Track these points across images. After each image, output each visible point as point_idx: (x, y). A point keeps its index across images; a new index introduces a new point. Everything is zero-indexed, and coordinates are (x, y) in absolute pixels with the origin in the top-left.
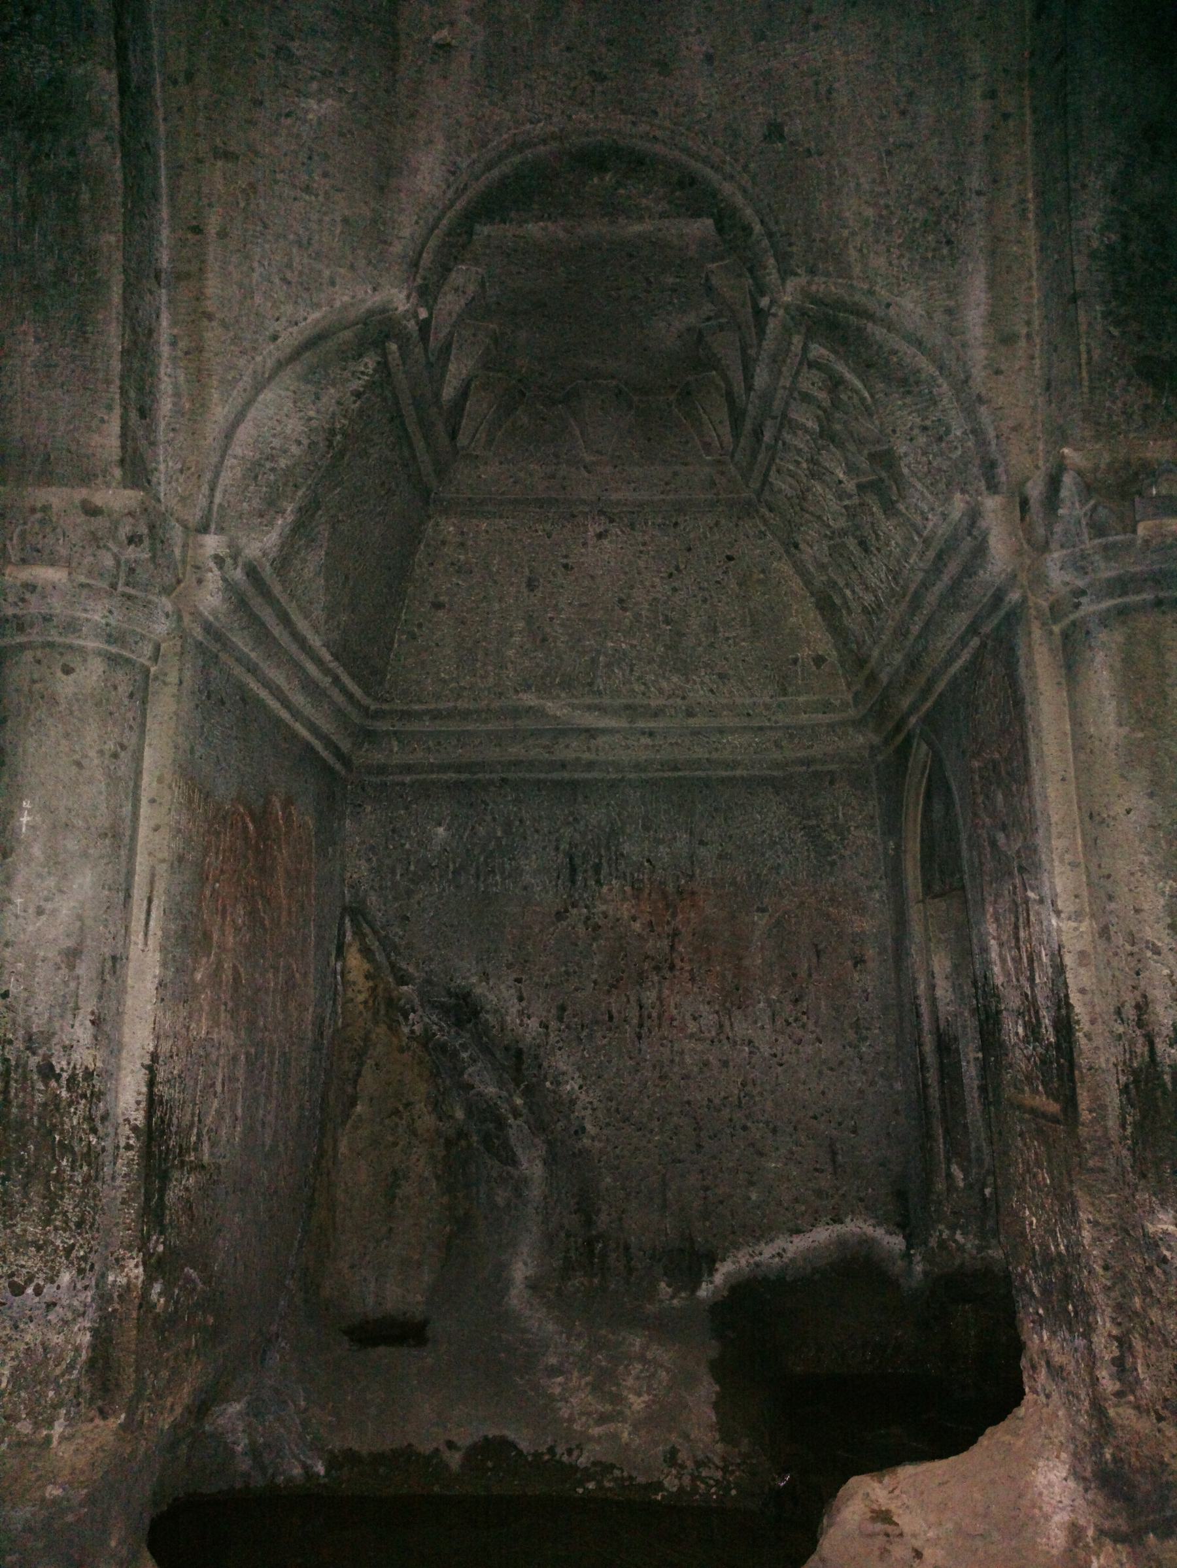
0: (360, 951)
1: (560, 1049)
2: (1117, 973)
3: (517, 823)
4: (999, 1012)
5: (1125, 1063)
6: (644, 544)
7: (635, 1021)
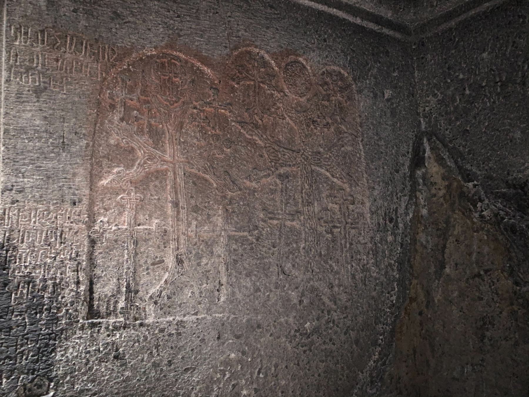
0: (436, 161)
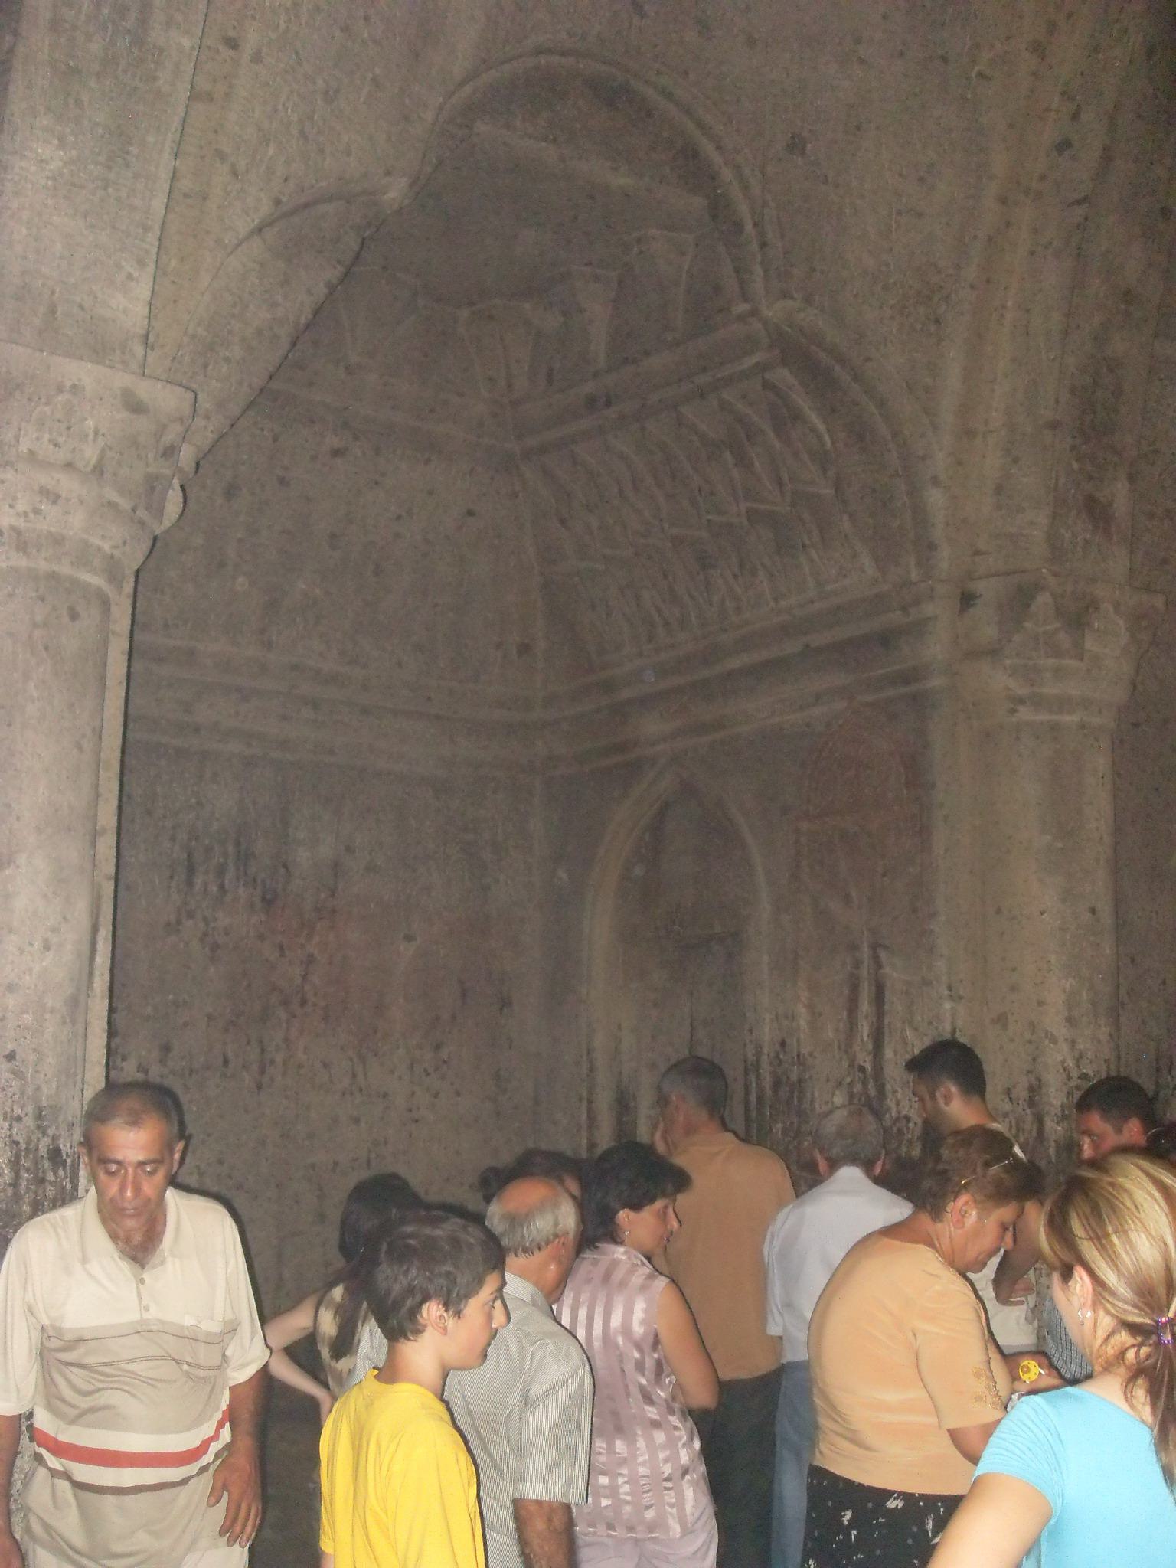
7: (255, 1067)
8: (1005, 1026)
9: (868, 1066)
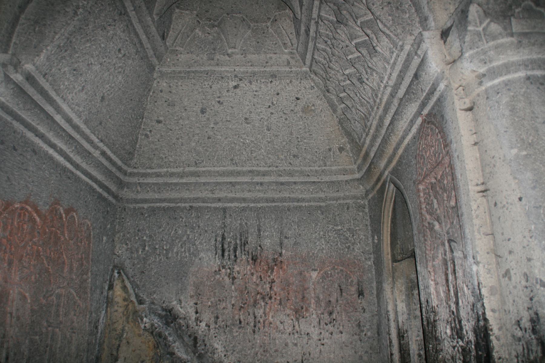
0: (122, 288)
1: (215, 337)
2: (516, 299)
3: (197, 228)
4: (435, 321)
5: (524, 356)
6: (256, 91)
7: (252, 324)
8: (510, 279)
9: (455, 310)
